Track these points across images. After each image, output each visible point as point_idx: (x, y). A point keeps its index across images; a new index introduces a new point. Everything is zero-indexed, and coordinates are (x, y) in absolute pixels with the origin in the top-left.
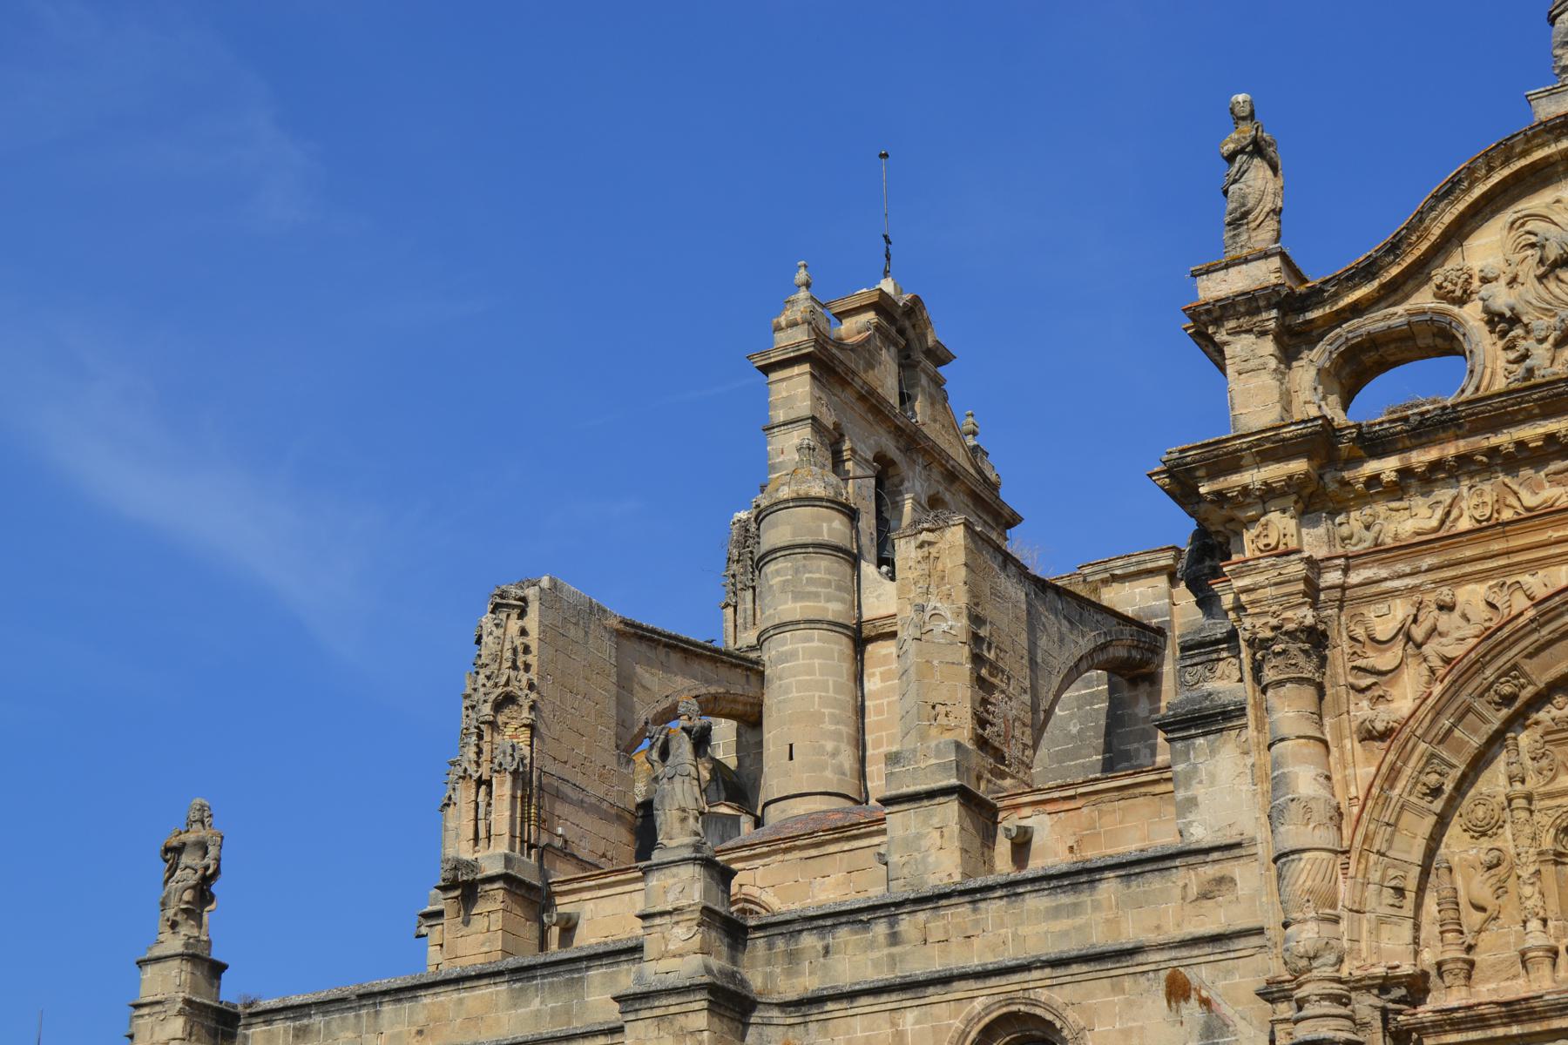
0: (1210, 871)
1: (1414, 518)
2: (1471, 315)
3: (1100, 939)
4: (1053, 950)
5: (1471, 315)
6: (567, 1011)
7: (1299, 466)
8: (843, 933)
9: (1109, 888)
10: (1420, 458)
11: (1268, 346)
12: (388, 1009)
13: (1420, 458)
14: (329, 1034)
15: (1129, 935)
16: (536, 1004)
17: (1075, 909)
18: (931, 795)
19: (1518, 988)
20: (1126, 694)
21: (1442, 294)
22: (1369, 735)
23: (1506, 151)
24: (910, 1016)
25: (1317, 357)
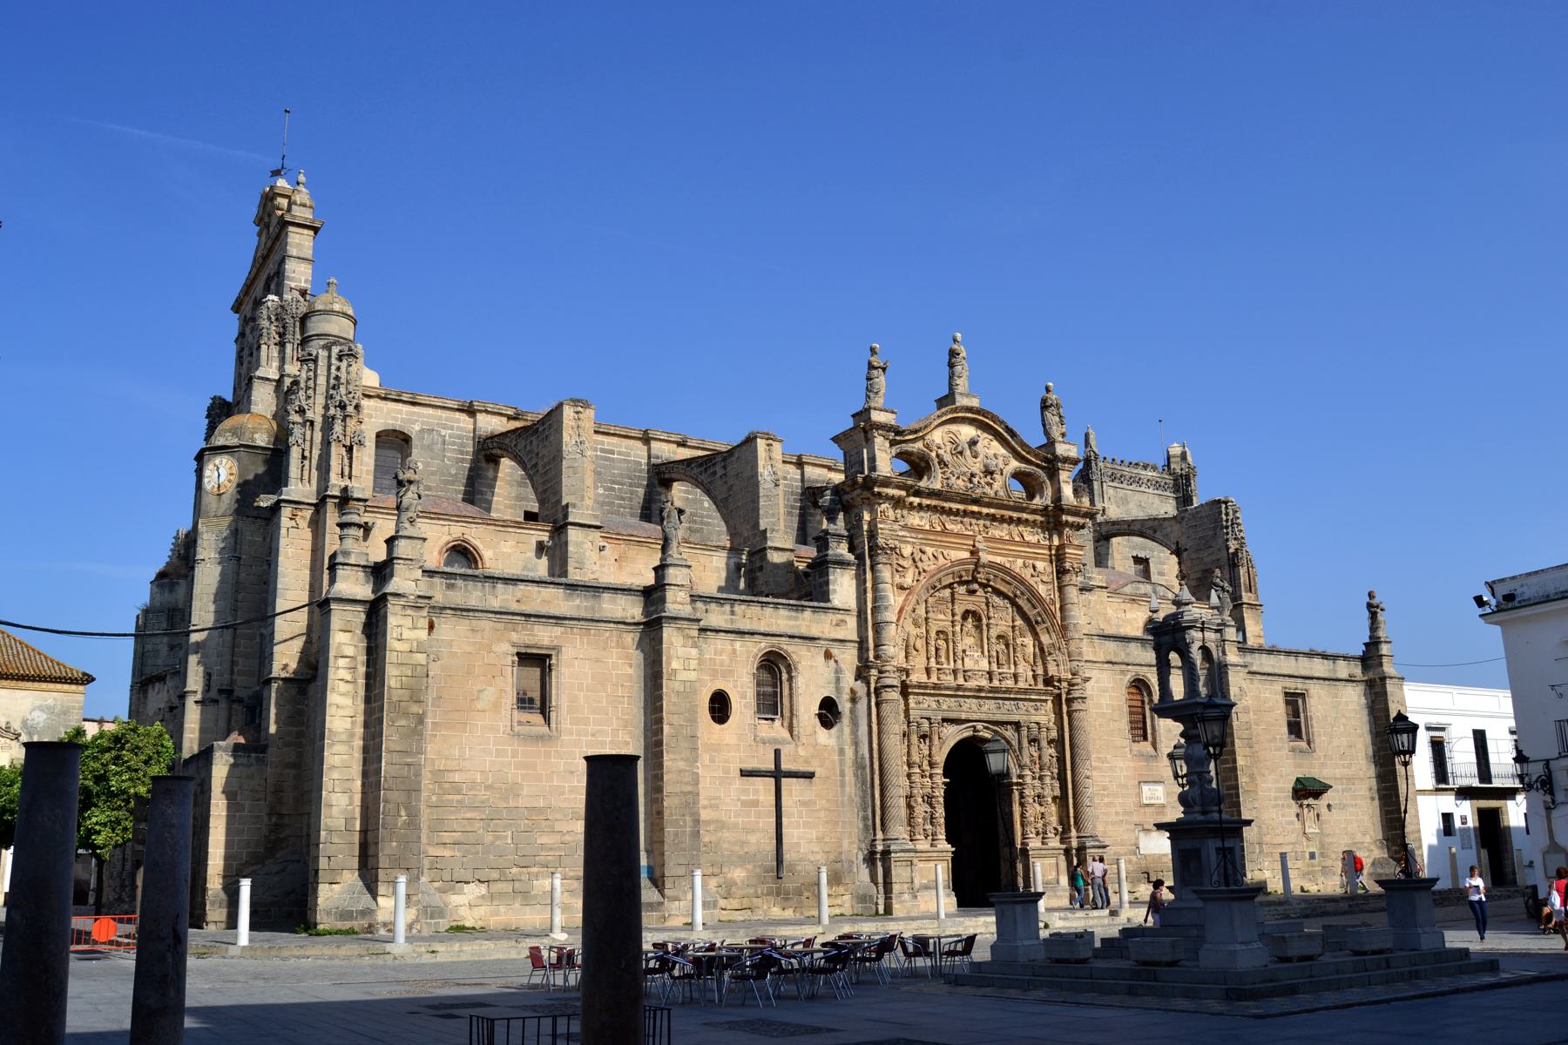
0: (840, 617)
1: (915, 519)
2: (933, 454)
3: (804, 632)
4: (790, 632)
5: (933, 454)
6: (593, 608)
7: (903, 493)
8: (713, 606)
9: (808, 614)
10: (926, 502)
11: (887, 444)
12: (500, 586)
13: (926, 502)
14: (467, 591)
15: (814, 632)
16: (577, 602)
17: (796, 619)
18: (590, 526)
19: (924, 678)
20: (484, 464)
21: (927, 446)
22: (902, 588)
23: (1008, 430)
24: (738, 645)
25: (894, 450)
